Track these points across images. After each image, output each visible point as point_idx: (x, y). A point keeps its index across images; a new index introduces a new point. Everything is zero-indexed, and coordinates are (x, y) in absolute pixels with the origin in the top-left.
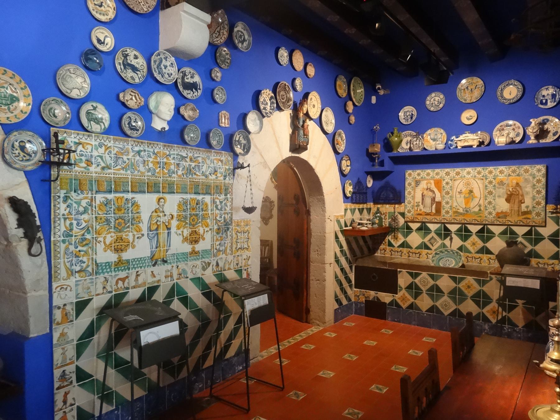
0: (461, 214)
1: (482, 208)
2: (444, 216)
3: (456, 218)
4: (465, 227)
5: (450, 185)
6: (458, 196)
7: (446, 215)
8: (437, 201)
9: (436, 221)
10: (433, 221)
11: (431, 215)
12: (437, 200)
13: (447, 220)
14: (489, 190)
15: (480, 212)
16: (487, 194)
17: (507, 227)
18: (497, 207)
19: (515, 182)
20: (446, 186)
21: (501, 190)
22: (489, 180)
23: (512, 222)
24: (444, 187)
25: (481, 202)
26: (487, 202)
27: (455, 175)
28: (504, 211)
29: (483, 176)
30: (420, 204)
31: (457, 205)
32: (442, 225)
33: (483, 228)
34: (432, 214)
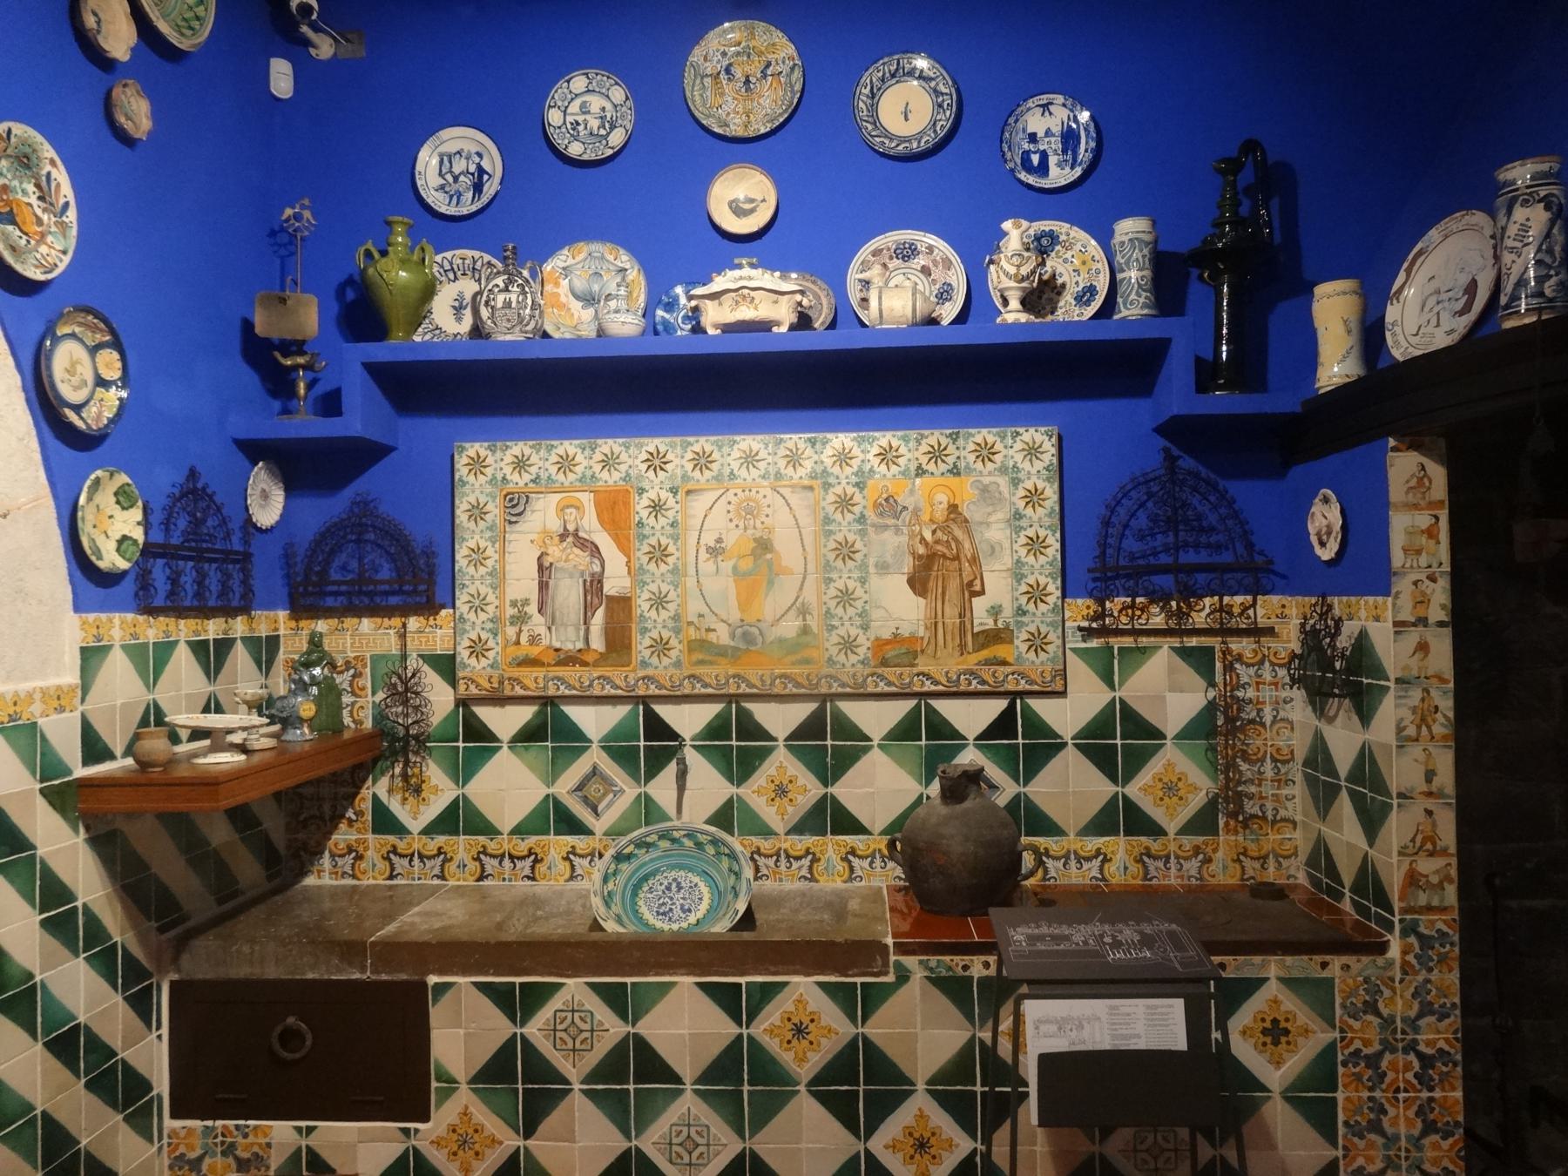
0: (721, 652)
1: (813, 623)
2: (644, 664)
3: (699, 671)
4: (740, 710)
5: (670, 514)
6: (707, 566)
7: (655, 660)
8: (612, 592)
9: (609, 690)
10: (597, 691)
11: (584, 664)
12: (611, 587)
13: (660, 687)
14: (840, 537)
15: (809, 639)
16: (832, 556)
17: (918, 706)
18: (876, 614)
19: (942, 498)
20: (652, 521)
21: (888, 535)
22: (838, 490)
23: (937, 683)
24: (640, 524)
25: (810, 595)
26: (832, 592)
27: (689, 466)
28: (905, 631)
29: (813, 476)
30: (532, 609)
31: (705, 610)
32: (635, 713)
34: (589, 658)
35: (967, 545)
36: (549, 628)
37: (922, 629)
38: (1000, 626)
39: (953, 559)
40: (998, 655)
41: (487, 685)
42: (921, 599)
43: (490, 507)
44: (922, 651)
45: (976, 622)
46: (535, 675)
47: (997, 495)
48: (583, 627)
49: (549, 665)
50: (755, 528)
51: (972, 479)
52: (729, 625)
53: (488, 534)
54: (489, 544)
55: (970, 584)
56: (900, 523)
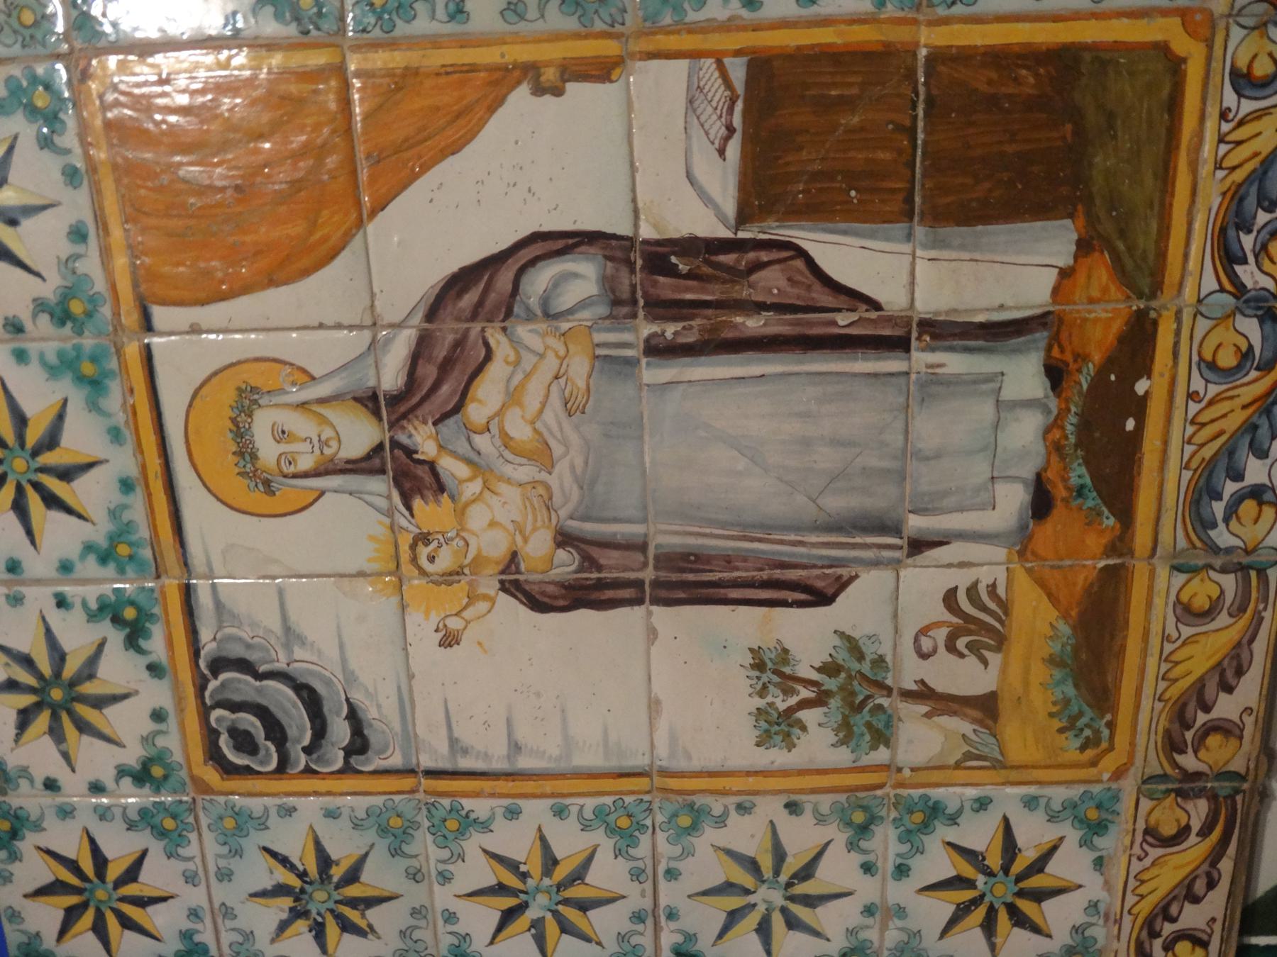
36: (918, 546)
41: (1194, 851)
46: (1163, 613)
48: (921, 358)
49: (1120, 545)
53: (425, 847)
54: (473, 843)
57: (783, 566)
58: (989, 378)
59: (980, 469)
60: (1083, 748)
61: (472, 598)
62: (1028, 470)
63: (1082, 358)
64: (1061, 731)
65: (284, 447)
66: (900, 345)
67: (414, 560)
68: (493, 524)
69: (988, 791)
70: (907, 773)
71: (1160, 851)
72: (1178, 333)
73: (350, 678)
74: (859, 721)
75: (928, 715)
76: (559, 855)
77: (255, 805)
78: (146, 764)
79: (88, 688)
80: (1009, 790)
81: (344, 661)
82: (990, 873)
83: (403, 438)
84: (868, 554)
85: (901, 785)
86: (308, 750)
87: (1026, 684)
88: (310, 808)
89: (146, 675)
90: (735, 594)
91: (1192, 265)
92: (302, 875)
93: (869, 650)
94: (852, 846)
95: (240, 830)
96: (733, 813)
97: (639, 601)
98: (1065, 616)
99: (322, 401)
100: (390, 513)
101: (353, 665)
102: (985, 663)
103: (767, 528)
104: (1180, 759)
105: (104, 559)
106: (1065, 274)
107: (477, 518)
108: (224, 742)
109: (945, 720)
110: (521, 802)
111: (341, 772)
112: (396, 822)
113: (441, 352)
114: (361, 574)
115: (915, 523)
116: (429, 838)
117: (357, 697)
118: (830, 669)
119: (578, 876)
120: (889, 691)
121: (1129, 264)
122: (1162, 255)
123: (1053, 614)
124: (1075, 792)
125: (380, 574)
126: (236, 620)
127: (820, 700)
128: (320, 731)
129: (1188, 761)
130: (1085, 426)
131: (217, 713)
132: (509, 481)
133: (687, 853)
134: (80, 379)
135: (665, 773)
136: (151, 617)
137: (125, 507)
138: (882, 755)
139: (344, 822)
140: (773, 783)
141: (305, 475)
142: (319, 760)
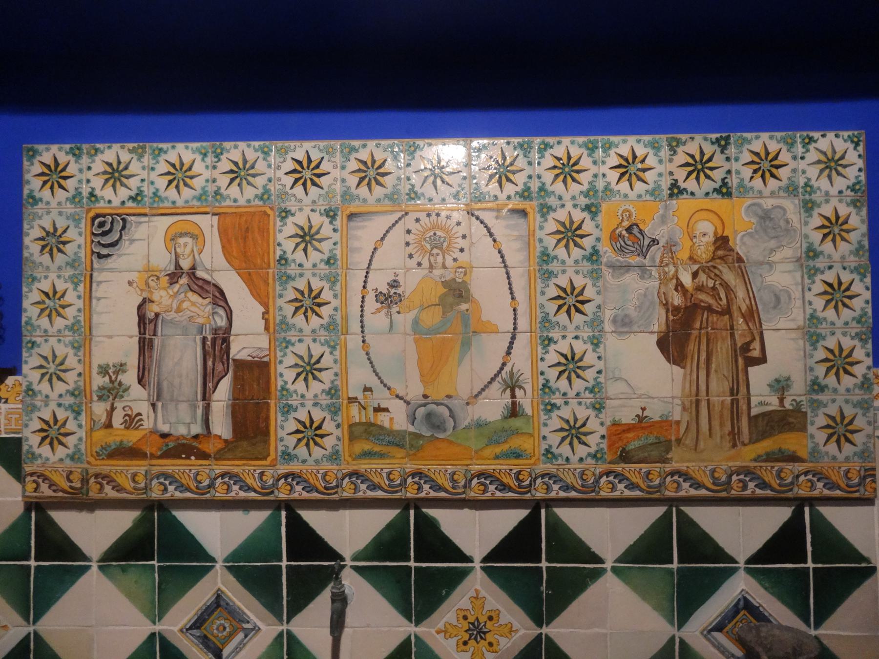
0: (396, 440)
1: (526, 402)
2: (287, 456)
3: (364, 466)
4: (420, 516)
5: (326, 246)
6: (377, 320)
7: (302, 451)
8: (243, 356)
9: (237, 493)
10: (220, 494)
11: (203, 456)
12: (240, 349)
13: (310, 488)
14: (563, 282)
15: (516, 423)
16: (552, 307)
17: (667, 516)
18: (613, 389)
19: (706, 228)
20: (299, 256)
21: (630, 278)
22: (561, 215)
23: (698, 485)
24: (283, 260)
25: (521, 361)
26: (553, 357)
27: (353, 180)
28: (654, 413)
29: (525, 194)
30: (130, 377)
31: (373, 382)
32: (274, 522)
33: (528, 528)
34: (211, 447)
35: (741, 293)
36: (154, 405)
37: (678, 410)
38: (788, 405)
39: (721, 313)
40: (784, 447)
41: (65, 485)
42: (675, 368)
43: (71, 234)
44: (679, 441)
45: (754, 401)
46: (133, 470)
47: (782, 223)
48: (201, 404)
49: (153, 456)
50: (444, 267)
51: (749, 202)
52: (408, 403)
53: (69, 272)
54: (70, 286)
55: (746, 347)
56: (647, 261)
57: (149, 371)
58: (196, 420)
59: (173, 420)
60: (96, 452)
61: (142, 290)
62: (172, 432)
63: (200, 443)
64: (102, 446)
65: (182, 245)
66: (204, 399)
67: (152, 276)
68: (161, 297)
69: (84, 428)
70: (90, 405)
71: (65, 476)
72: (206, 465)
73: (120, 256)
74: (105, 392)
75: (107, 410)
76: (66, 309)
77: (83, 225)
78: (95, 196)
79: (118, 184)
80: (84, 434)
81: (125, 254)
82: (59, 429)
83: (184, 275)
84: (152, 393)
85: (86, 403)
86: (99, 242)
87: (116, 435)
88: (81, 240)
89: (122, 200)
90: (141, 358)
91: (221, 467)
92: (60, 236)
93: (125, 394)
94: (68, 391)
95: (75, 220)
96: (78, 358)
97: (140, 333)
98: (134, 444)
99: (194, 256)
100: (165, 270)
101: (124, 257)
102: (122, 424)
103: (159, 366)
104: (93, 478)
105: (154, 194)
106: (220, 437)
107: (163, 293)
108: (102, 219)
109: (105, 415)
110: (82, 300)
111: (92, 250)
112: (77, 264)
113: (206, 287)
114: (149, 261)
115: (159, 404)
116: (72, 273)
117: (114, 257)
118: (120, 384)
119: (59, 315)
120: (114, 399)
121: (222, 452)
122: (224, 459)
123: (135, 440)
124: (83, 451)
125: (149, 266)
126: (137, 227)
127: (112, 381)
128: (104, 246)
129: (92, 480)
130: (183, 445)
131: (110, 218)
132: (172, 302)
133: (66, 346)
134: (201, 195)
135: (91, 340)
136: (138, 204)
137: (168, 201)
138: (95, 398)
139: (76, 250)
140: (87, 369)
141: (175, 250)
142: (95, 245)
